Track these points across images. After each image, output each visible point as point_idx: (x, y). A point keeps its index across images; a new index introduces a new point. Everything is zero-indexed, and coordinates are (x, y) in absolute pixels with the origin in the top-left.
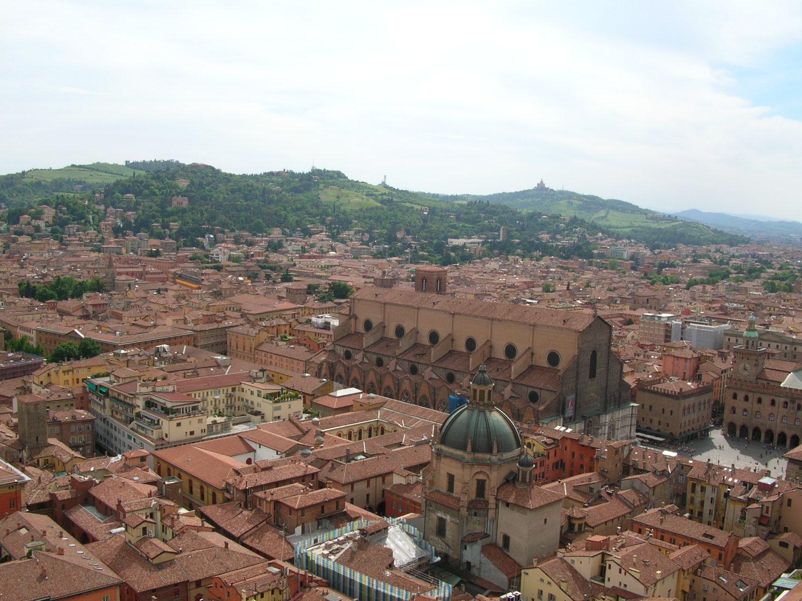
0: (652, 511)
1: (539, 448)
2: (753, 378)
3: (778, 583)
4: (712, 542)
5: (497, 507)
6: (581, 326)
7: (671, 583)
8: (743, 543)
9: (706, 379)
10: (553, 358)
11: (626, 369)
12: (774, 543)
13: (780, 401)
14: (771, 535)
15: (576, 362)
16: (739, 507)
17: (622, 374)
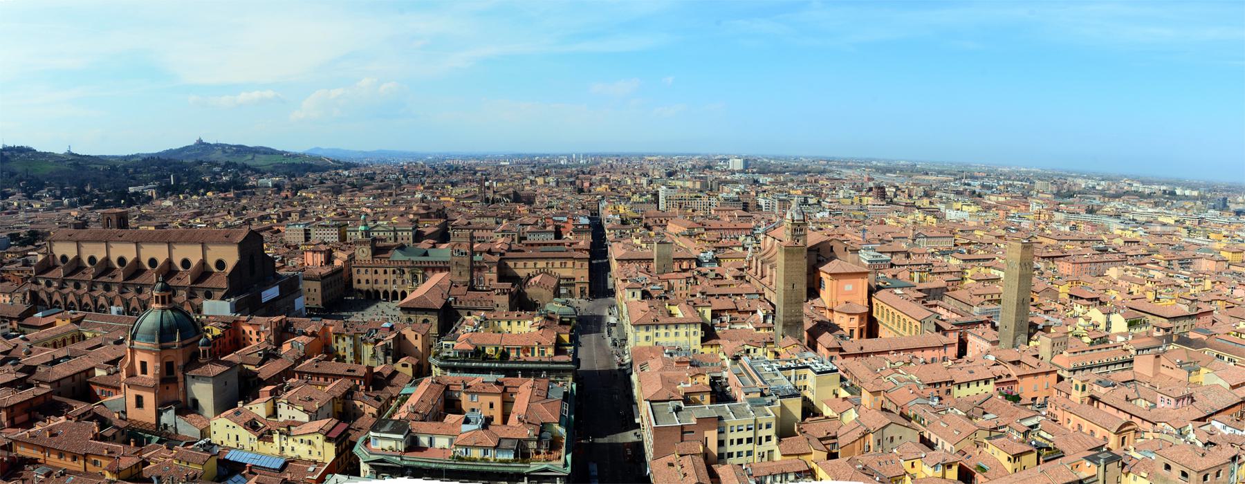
0: (308, 361)
1: (217, 332)
2: (370, 258)
3: (404, 392)
4: (356, 374)
5: (185, 379)
6: (240, 238)
7: (329, 409)
8: (375, 370)
9: (338, 263)
10: (220, 264)
11: (278, 265)
12: (398, 366)
13: (390, 270)
14: (395, 361)
15: (238, 266)
16: (371, 347)
17: (275, 268)
